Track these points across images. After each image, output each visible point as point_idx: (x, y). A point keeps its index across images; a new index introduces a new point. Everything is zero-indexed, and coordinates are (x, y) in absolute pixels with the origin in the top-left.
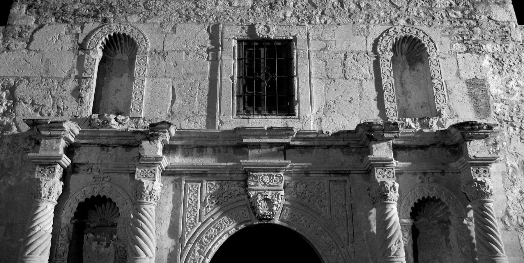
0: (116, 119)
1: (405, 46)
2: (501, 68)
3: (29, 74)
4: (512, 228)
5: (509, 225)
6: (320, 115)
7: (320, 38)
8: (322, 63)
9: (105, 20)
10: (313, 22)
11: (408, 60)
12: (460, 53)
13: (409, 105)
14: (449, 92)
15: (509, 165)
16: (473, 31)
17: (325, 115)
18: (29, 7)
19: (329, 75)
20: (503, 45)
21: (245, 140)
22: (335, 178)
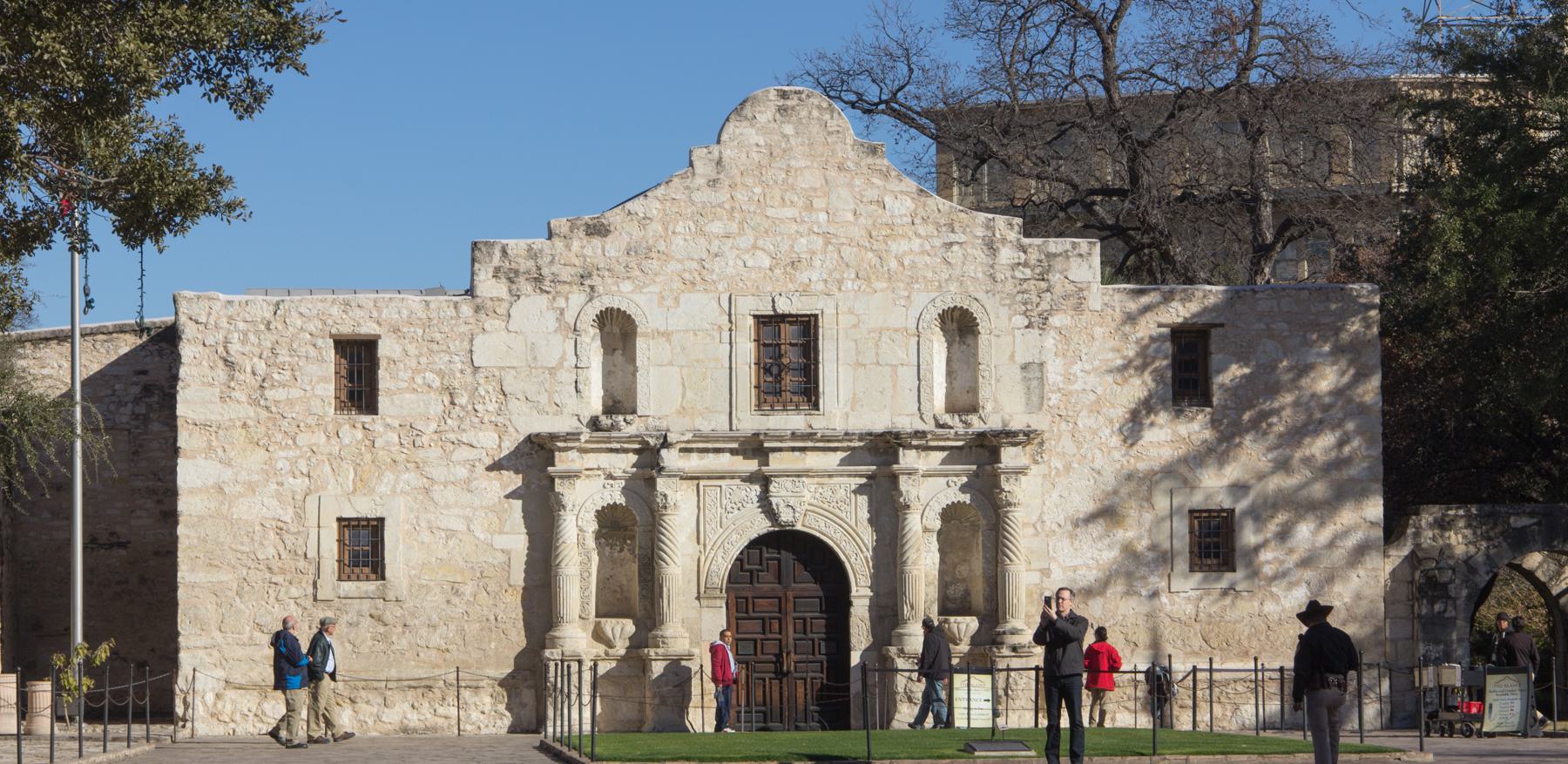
0: (625, 420)
1: (956, 314)
2: (1066, 347)
3: (515, 365)
4: (1043, 534)
5: (1040, 530)
6: (848, 409)
7: (851, 311)
8: (852, 344)
9: (592, 288)
10: (843, 288)
11: (960, 330)
12: (1019, 329)
13: (953, 388)
14: (998, 381)
17: (853, 410)
18: (497, 270)
21: (766, 445)
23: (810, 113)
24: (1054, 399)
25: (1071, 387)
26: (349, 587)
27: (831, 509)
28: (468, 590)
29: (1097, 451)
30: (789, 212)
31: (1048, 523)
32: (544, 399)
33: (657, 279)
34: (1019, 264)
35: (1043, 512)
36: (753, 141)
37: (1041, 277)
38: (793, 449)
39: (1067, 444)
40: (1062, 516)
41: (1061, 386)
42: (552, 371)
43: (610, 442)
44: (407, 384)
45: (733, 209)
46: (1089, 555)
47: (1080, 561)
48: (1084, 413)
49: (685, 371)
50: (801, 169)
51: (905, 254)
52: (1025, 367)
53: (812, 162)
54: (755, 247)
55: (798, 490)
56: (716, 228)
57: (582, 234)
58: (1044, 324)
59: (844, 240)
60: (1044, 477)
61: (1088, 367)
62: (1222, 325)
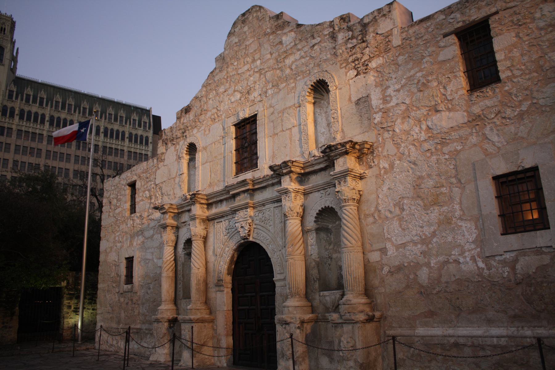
10: (267, 95)
15: (381, 166)
16: (362, 53)
19: (275, 131)
20: (385, 56)
22: (276, 205)
23: (253, 16)
24: (378, 118)
25: (388, 105)
26: (126, 286)
27: (264, 225)
28: (151, 286)
29: (411, 147)
30: (246, 68)
31: (383, 211)
32: (171, 193)
33: (204, 123)
34: (349, 39)
35: (378, 204)
36: (234, 42)
37: (362, 41)
38: (244, 192)
39: (390, 148)
40: (391, 205)
41: (381, 106)
42: (174, 178)
43: (183, 207)
44: (141, 198)
45: (227, 77)
46: (414, 233)
47: (408, 239)
48: (399, 121)
49: (211, 163)
50: (251, 44)
51: (293, 62)
52: (357, 103)
53: (254, 38)
54: (235, 91)
55: (246, 216)
56: (222, 89)
57: (183, 114)
58: (366, 69)
59: (267, 70)
60: (378, 176)
61: (397, 87)
62: (496, 13)
